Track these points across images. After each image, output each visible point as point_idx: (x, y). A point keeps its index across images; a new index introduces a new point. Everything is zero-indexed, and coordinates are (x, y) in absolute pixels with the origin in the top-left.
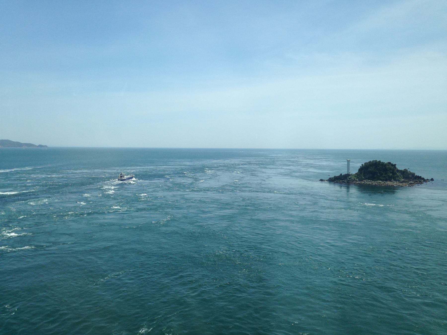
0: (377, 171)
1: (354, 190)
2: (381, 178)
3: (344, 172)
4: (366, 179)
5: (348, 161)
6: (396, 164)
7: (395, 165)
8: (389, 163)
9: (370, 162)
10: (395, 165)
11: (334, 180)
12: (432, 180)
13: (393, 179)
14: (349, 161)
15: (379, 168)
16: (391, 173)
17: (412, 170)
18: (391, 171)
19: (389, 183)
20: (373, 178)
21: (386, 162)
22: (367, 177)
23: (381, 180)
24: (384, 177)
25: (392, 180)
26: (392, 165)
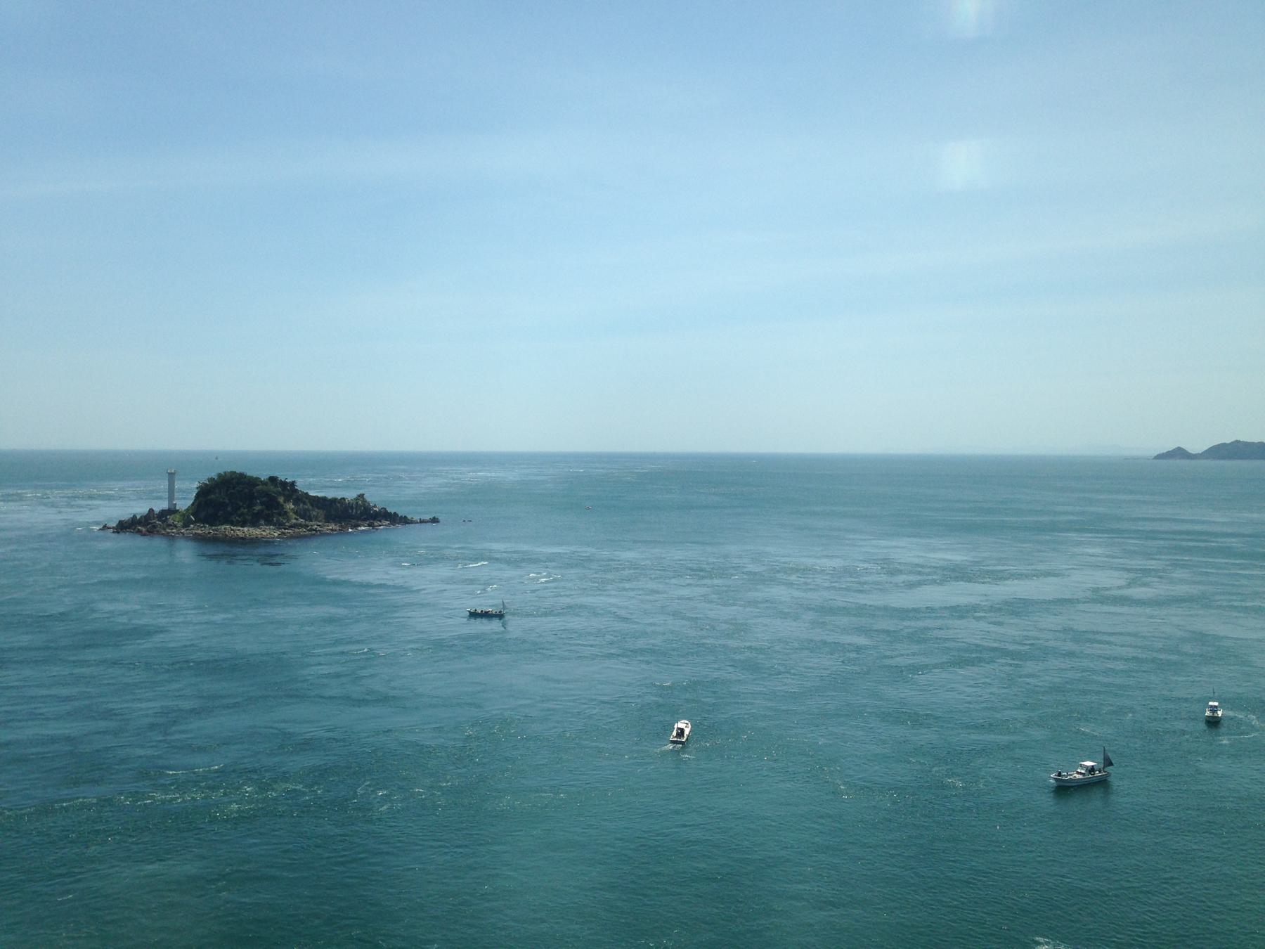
0: (227, 501)
1: (186, 554)
2: (234, 518)
3: (160, 505)
4: (198, 520)
5: (171, 476)
6: (294, 482)
7: (293, 483)
8: (273, 480)
9: (220, 475)
10: (293, 483)
11: (125, 527)
12: (435, 520)
13: (266, 520)
14: (173, 474)
15: (233, 491)
16: (262, 503)
17: (376, 498)
18: (264, 499)
19: (247, 531)
20: (212, 520)
21: (264, 476)
22: (202, 515)
23: (232, 524)
24: (242, 514)
25: (263, 522)
26: (284, 484)
